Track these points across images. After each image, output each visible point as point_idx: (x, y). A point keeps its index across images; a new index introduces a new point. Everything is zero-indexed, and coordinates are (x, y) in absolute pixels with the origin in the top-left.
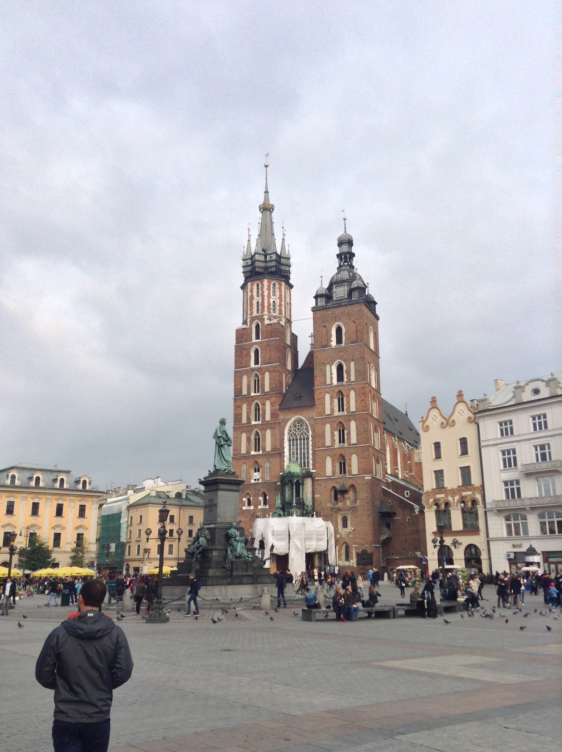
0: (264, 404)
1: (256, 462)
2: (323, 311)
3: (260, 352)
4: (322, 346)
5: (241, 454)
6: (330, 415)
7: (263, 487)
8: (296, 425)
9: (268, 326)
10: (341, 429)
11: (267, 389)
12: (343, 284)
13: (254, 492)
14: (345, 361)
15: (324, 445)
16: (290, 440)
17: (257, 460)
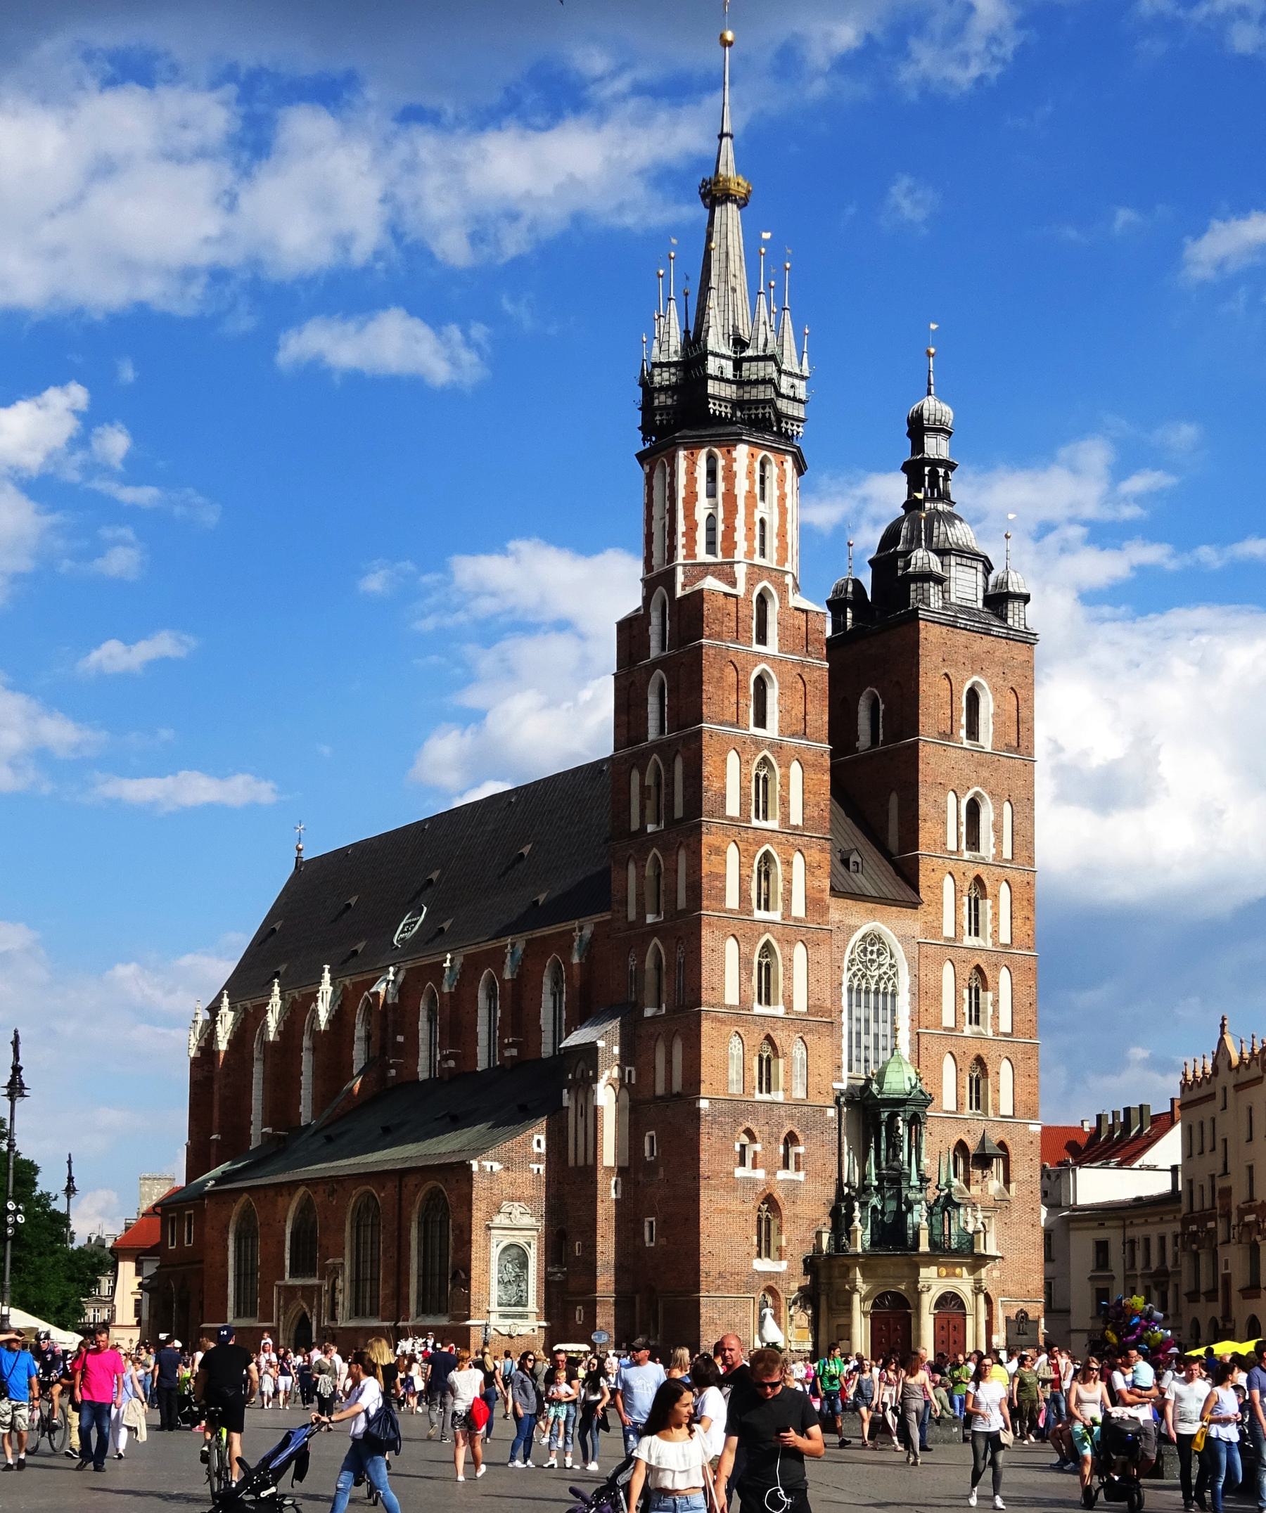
0: (788, 863)
1: (768, 1038)
2: (944, 629)
3: (773, 694)
4: (940, 733)
5: (725, 1006)
6: (954, 940)
7: (791, 1117)
8: (865, 948)
9: (797, 613)
10: (974, 985)
11: (796, 818)
12: (974, 564)
13: (766, 1128)
14: (992, 794)
15: (938, 1024)
16: (850, 990)
17: (772, 1034)
